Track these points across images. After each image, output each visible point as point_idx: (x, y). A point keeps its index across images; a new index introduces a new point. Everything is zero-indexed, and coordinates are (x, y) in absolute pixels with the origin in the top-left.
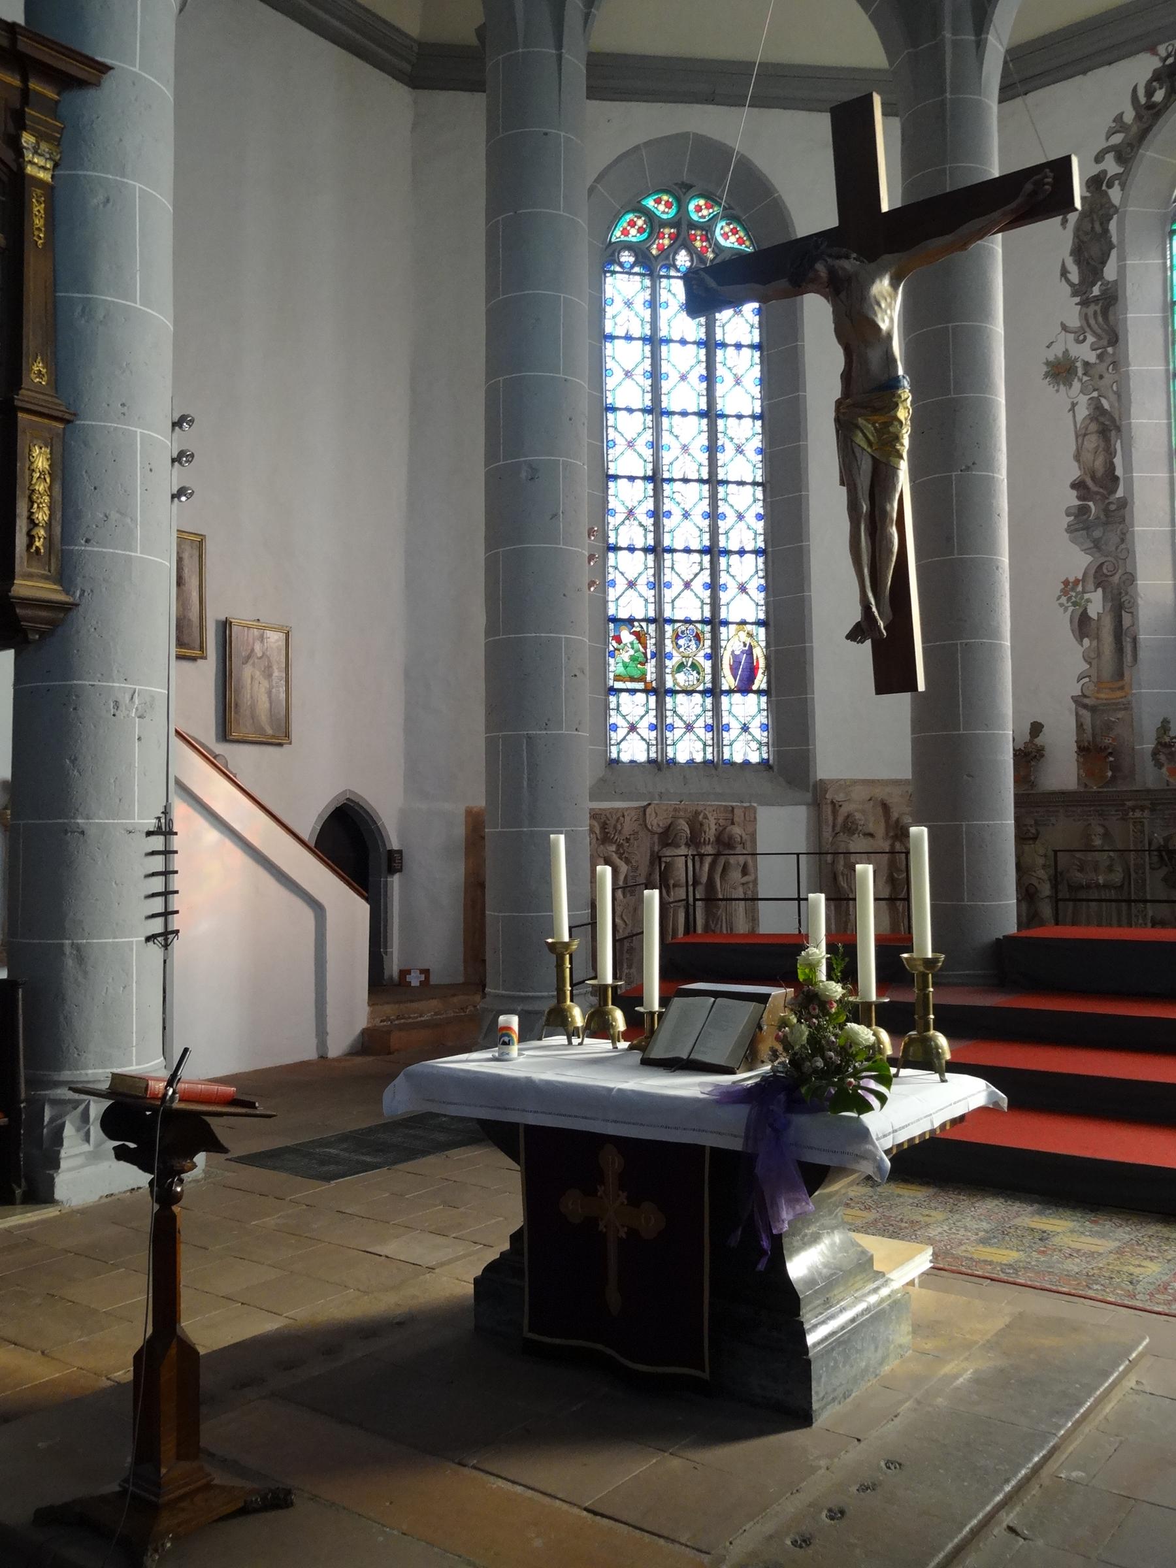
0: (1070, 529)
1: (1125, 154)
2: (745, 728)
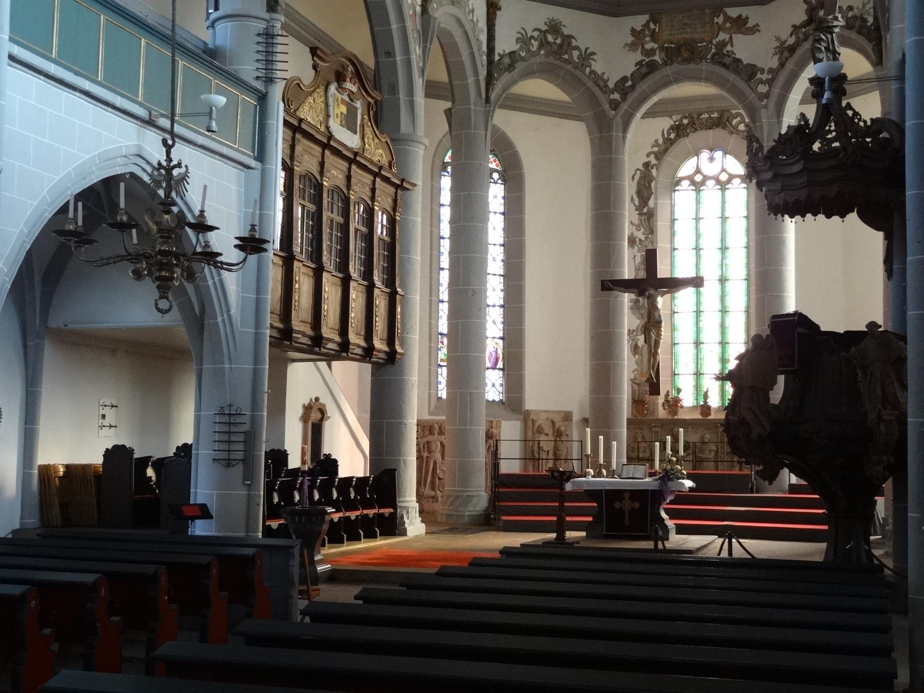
0: (631, 308)
1: (659, 156)
2: (493, 385)
